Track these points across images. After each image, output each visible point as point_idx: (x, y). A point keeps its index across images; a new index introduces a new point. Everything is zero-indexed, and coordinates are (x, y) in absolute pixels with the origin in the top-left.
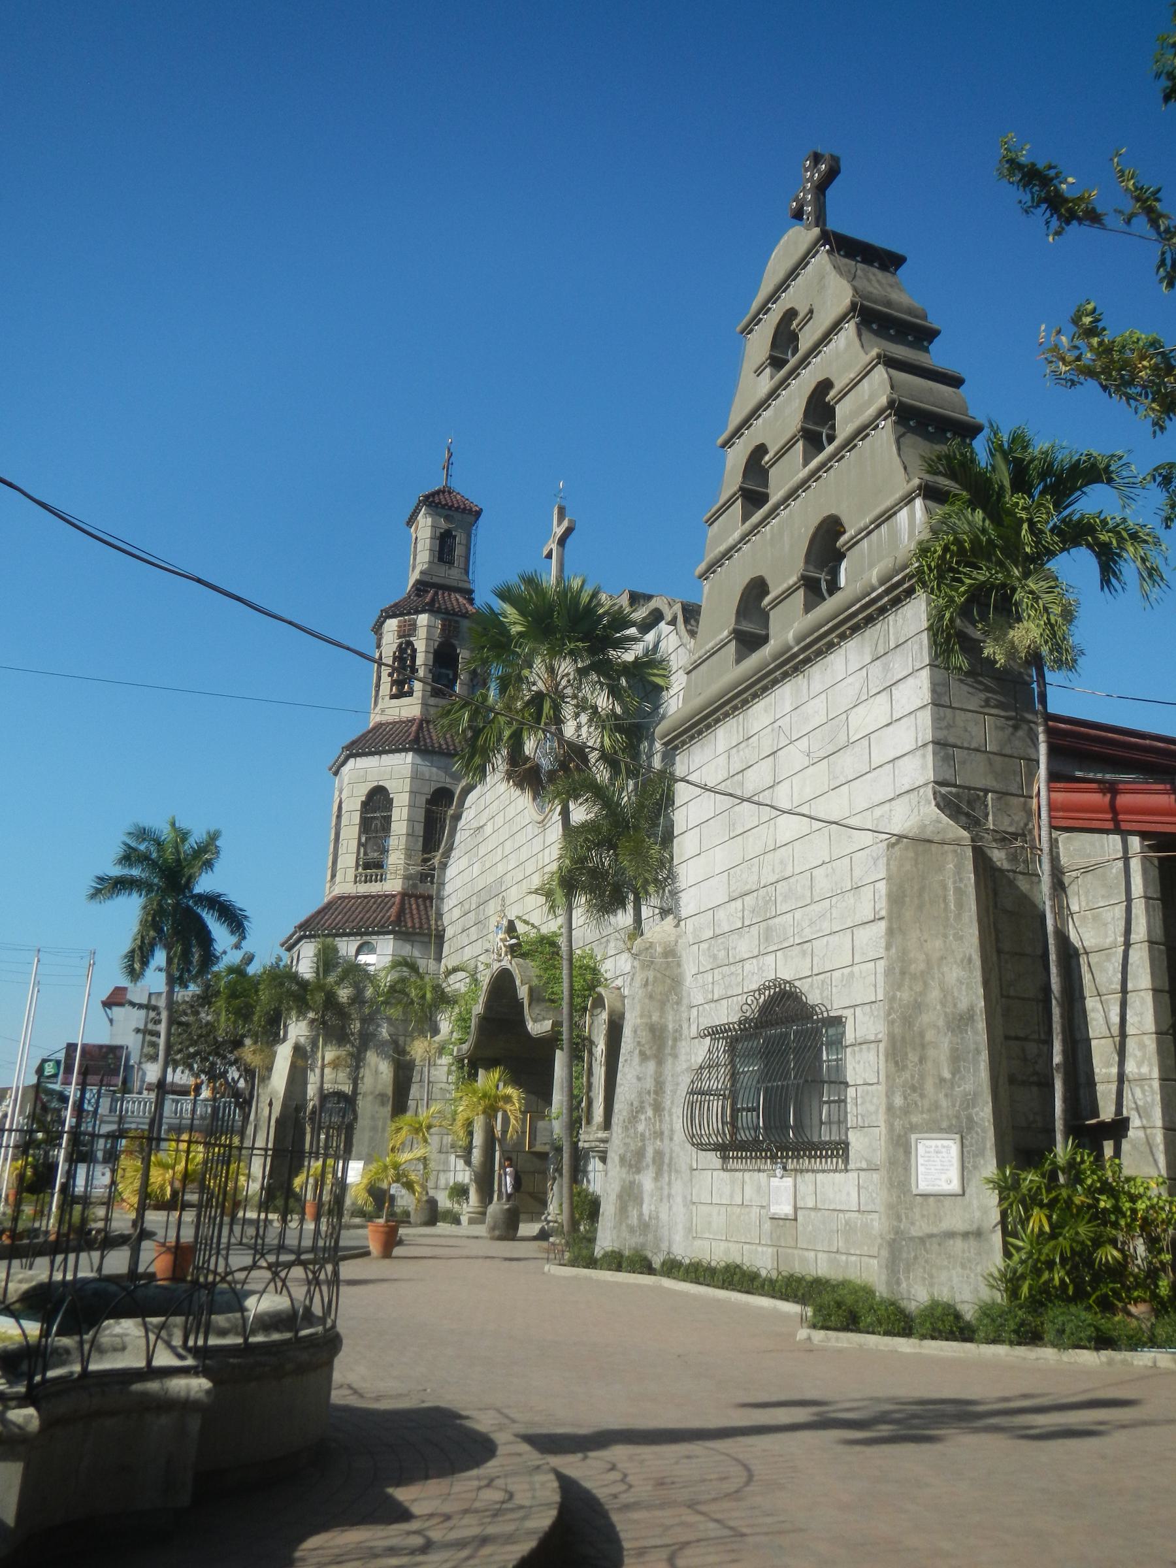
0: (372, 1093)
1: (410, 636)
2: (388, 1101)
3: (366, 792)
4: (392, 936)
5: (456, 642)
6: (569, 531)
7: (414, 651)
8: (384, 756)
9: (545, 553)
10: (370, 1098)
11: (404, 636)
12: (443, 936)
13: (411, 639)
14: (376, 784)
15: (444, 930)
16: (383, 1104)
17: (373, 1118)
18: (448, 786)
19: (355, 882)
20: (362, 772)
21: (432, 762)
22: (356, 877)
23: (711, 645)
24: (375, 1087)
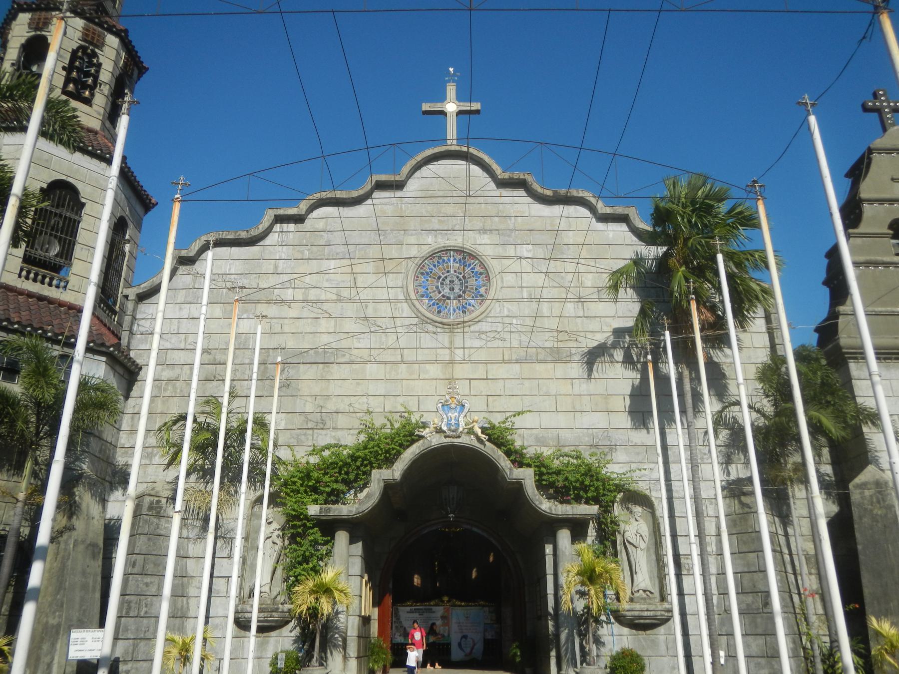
0: (83, 542)
1: (97, 46)
2: (99, 553)
3: (49, 181)
4: (104, 359)
5: (128, 82)
6: (477, 112)
7: (99, 65)
8: (78, 155)
9: (426, 107)
10: (81, 548)
11: (91, 43)
12: (138, 374)
13: (97, 50)
14: (64, 178)
15: (141, 368)
16: (94, 556)
17: (84, 573)
18: (127, 218)
19: (20, 276)
20: (46, 156)
21: (123, 187)
22: (22, 270)
23: (880, 309)
24: (86, 535)
